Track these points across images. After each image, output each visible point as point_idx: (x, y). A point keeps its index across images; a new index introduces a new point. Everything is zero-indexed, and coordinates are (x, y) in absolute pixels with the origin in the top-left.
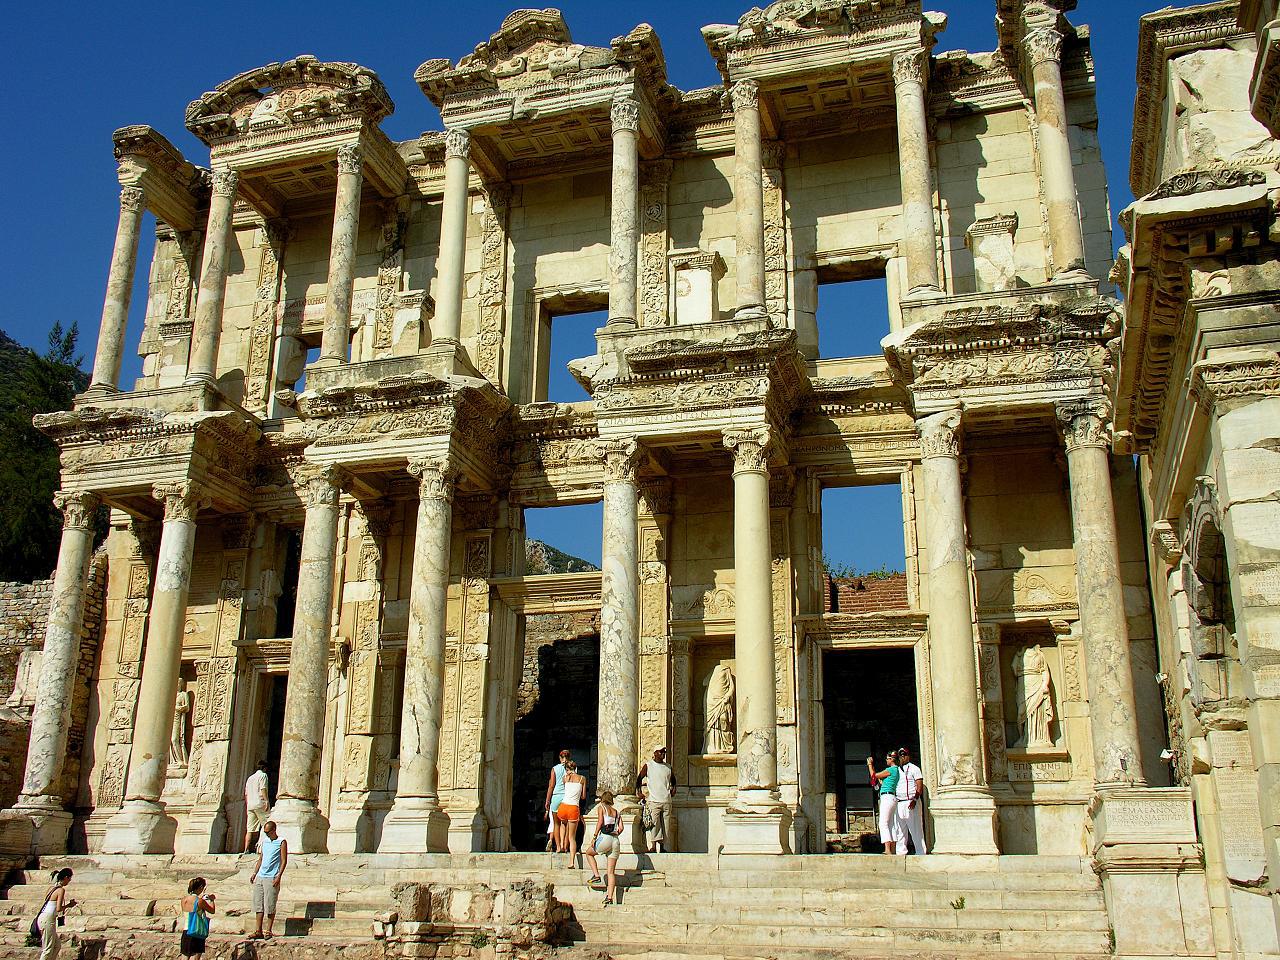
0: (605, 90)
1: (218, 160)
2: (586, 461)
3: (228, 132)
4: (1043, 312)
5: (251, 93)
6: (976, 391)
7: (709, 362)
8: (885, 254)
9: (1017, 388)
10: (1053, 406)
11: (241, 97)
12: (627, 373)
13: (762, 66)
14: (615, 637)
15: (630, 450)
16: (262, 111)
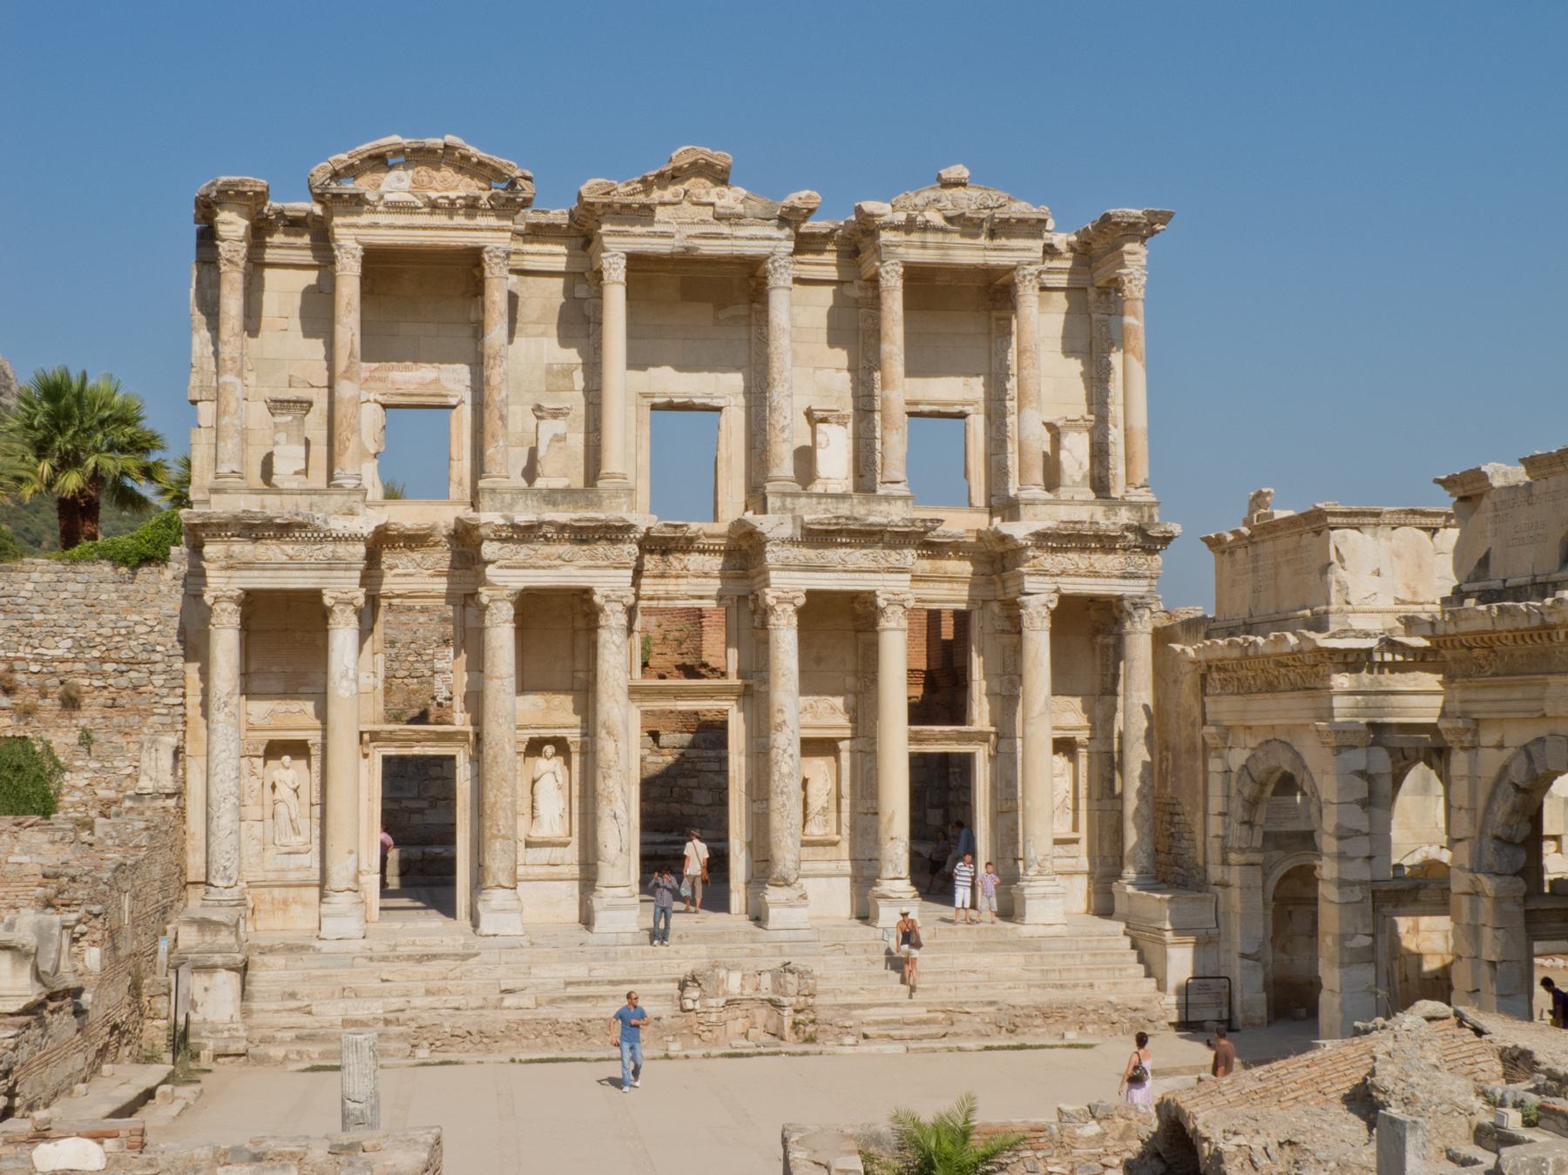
0: (766, 243)
1: (344, 231)
2: (706, 575)
3: (357, 202)
4: (1128, 528)
5: (379, 161)
6: (1069, 580)
7: (869, 536)
8: (967, 409)
9: (1099, 581)
10: (1120, 598)
11: (371, 163)
12: (799, 532)
13: (911, 251)
14: (788, 759)
15: (801, 601)
16: (396, 184)
